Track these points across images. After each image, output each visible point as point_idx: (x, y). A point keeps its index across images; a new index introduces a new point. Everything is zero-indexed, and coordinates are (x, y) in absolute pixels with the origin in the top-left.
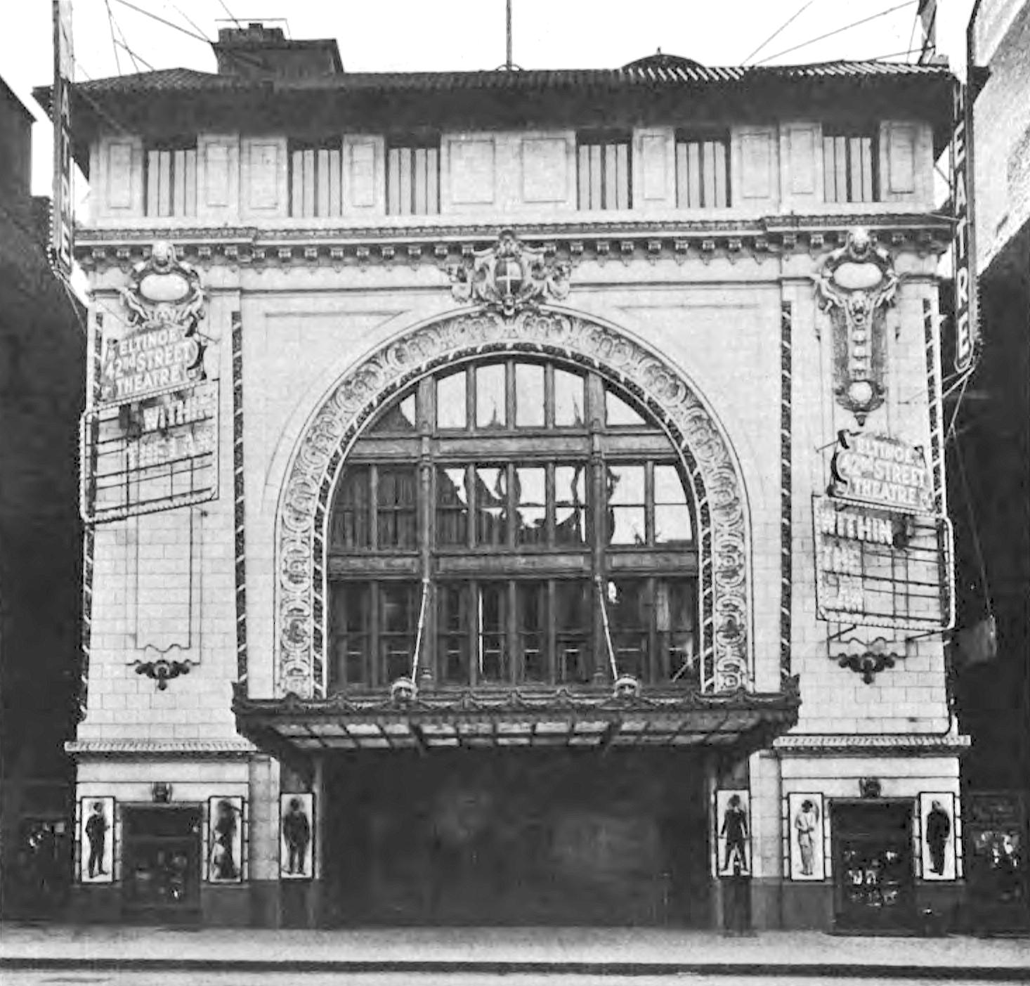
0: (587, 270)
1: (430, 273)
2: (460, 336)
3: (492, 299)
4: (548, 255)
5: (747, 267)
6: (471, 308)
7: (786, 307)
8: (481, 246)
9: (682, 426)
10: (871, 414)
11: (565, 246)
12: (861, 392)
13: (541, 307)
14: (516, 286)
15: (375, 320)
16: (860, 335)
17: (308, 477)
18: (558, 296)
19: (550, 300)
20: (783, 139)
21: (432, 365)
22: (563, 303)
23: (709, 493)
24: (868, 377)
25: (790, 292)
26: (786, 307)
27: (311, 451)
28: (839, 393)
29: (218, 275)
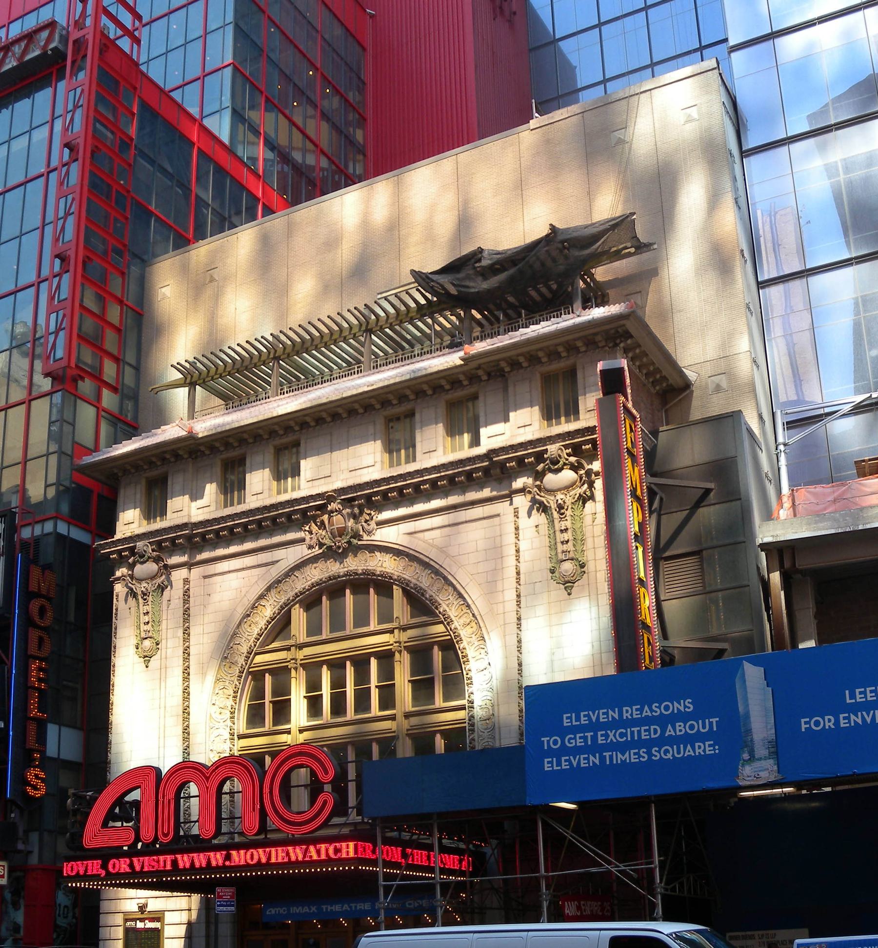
2: (314, 572)
4: (361, 507)
6: (317, 551)
12: (568, 566)
13: (360, 543)
14: (342, 532)
16: (563, 525)
17: (227, 684)
18: (369, 533)
19: (365, 537)
20: (511, 389)
21: (297, 595)
22: (373, 538)
24: (572, 555)
27: (228, 665)
28: (552, 571)
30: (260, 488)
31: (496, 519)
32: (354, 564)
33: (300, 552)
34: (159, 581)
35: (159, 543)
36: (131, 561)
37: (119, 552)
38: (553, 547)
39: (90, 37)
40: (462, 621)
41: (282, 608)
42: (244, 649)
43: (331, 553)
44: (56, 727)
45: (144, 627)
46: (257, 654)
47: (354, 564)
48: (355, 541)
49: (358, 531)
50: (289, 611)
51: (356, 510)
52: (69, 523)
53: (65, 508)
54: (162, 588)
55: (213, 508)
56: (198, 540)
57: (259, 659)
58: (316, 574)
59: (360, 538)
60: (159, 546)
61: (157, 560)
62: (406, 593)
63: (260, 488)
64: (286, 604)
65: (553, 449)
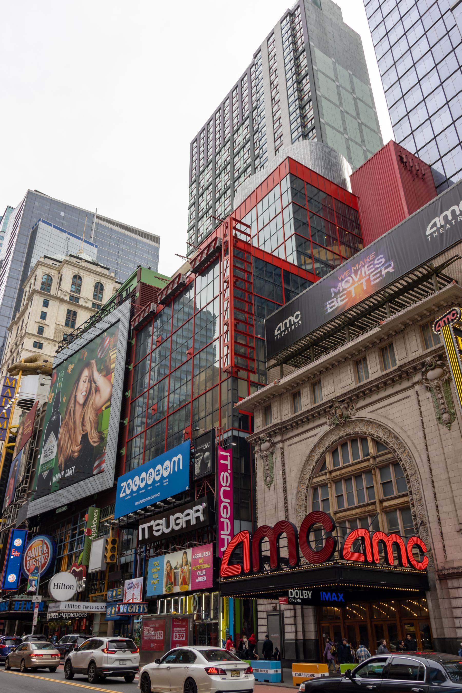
0: (361, 403)
1: (323, 420)
2: (333, 436)
3: (337, 422)
4: (348, 403)
5: (406, 384)
6: (333, 427)
7: (417, 393)
8: (331, 407)
9: (395, 448)
10: (452, 424)
11: (352, 398)
14: (341, 416)
15: (311, 439)
19: (352, 417)
21: (327, 449)
23: (408, 470)
25: (417, 387)
26: (417, 393)
29: (278, 438)
30: (306, 403)
31: (409, 398)
32: (349, 430)
33: (326, 428)
34: (271, 450)
35: (269, 433)
36: (259, 443)
37: (255, 440)
38: (437, 407)
39: (229, 240)
40: (400, 451)
41: (321, 455)
42: (308, 477)
43: (338, 426)
44: (239, 521)
45: (268, 471)
46: (313, 478)
47: (349, 430)
48: (347, 420)
49: (348, 414)
50: (325, 456)
51: (346, 405)
52: (239, 431)
53: (236, 425)
54: (272, 453)
55: (290, 415)
56: (284, 429)
57: (315, 480)
58: (333, 438)
59: (349, 417)
60: (270, 435)
61: (269, 441)
62: (373, 440)
63: (306, 403)
64: (323, 453)
65: (428, 359)
